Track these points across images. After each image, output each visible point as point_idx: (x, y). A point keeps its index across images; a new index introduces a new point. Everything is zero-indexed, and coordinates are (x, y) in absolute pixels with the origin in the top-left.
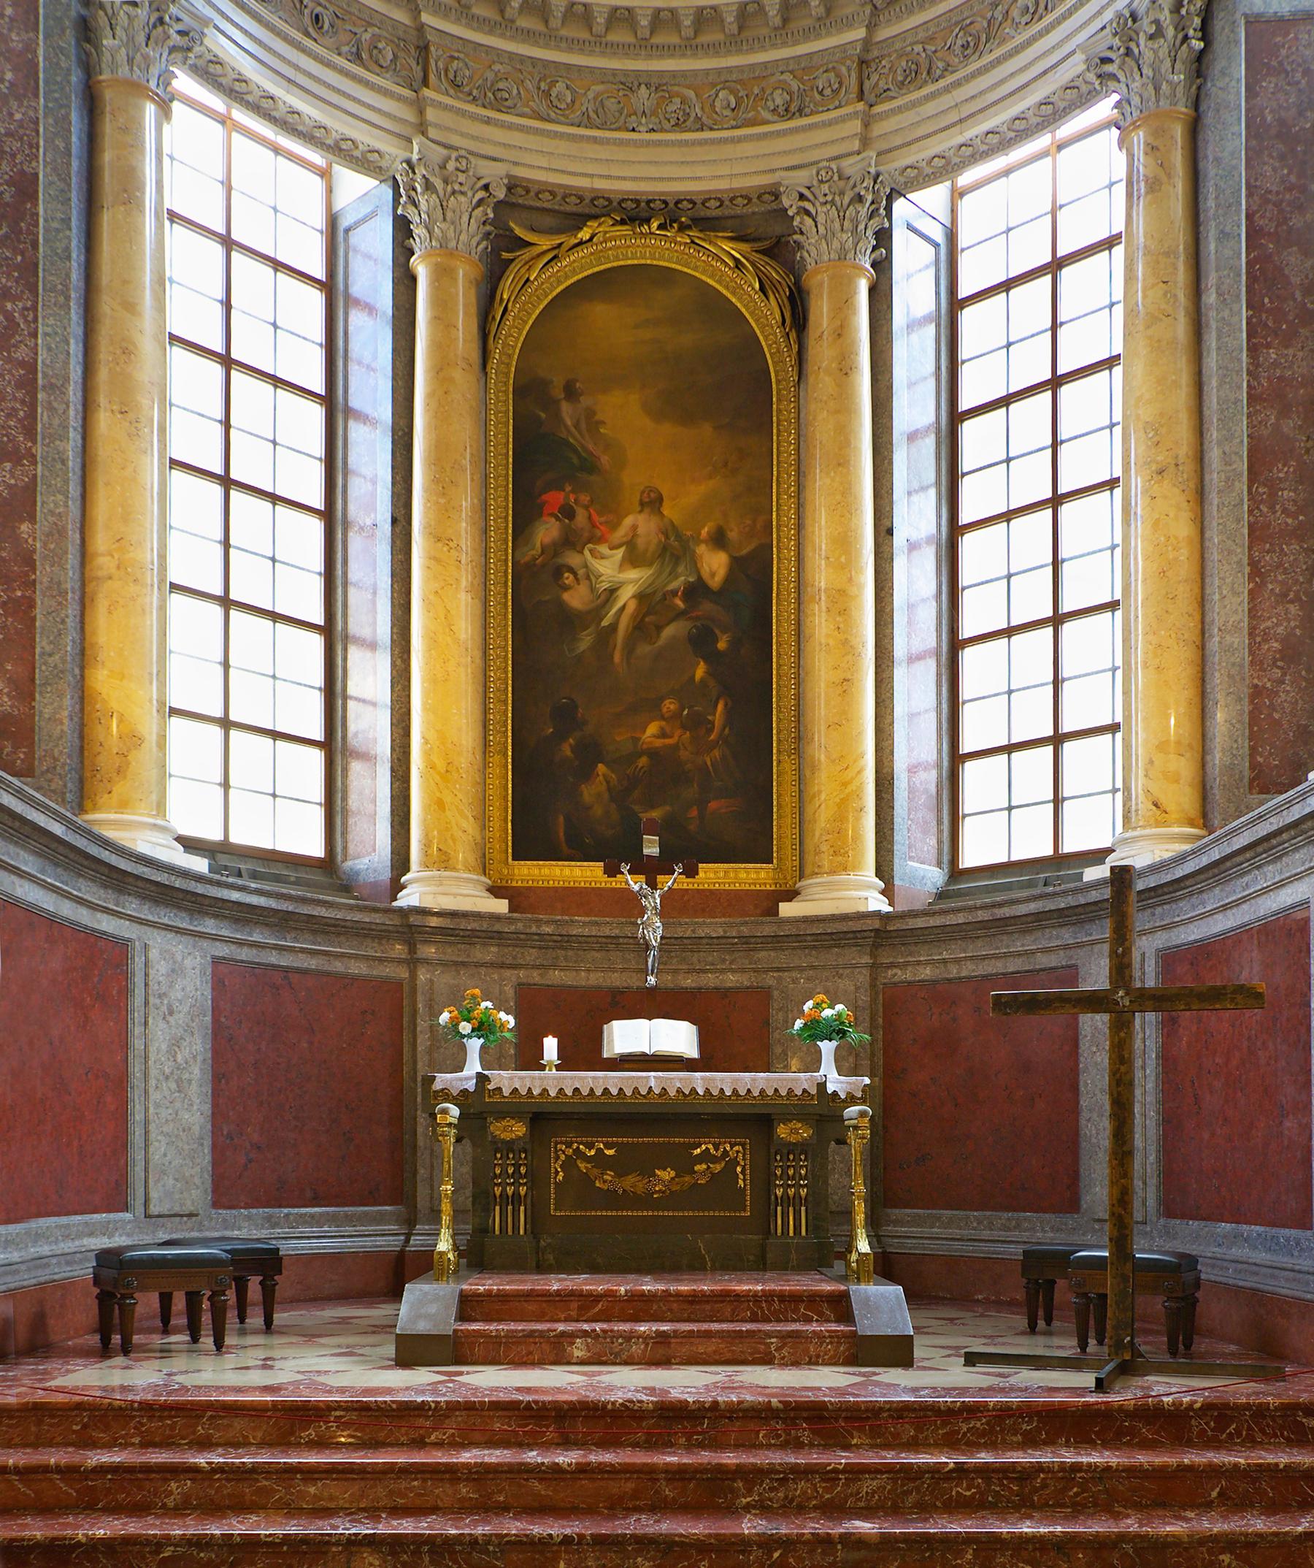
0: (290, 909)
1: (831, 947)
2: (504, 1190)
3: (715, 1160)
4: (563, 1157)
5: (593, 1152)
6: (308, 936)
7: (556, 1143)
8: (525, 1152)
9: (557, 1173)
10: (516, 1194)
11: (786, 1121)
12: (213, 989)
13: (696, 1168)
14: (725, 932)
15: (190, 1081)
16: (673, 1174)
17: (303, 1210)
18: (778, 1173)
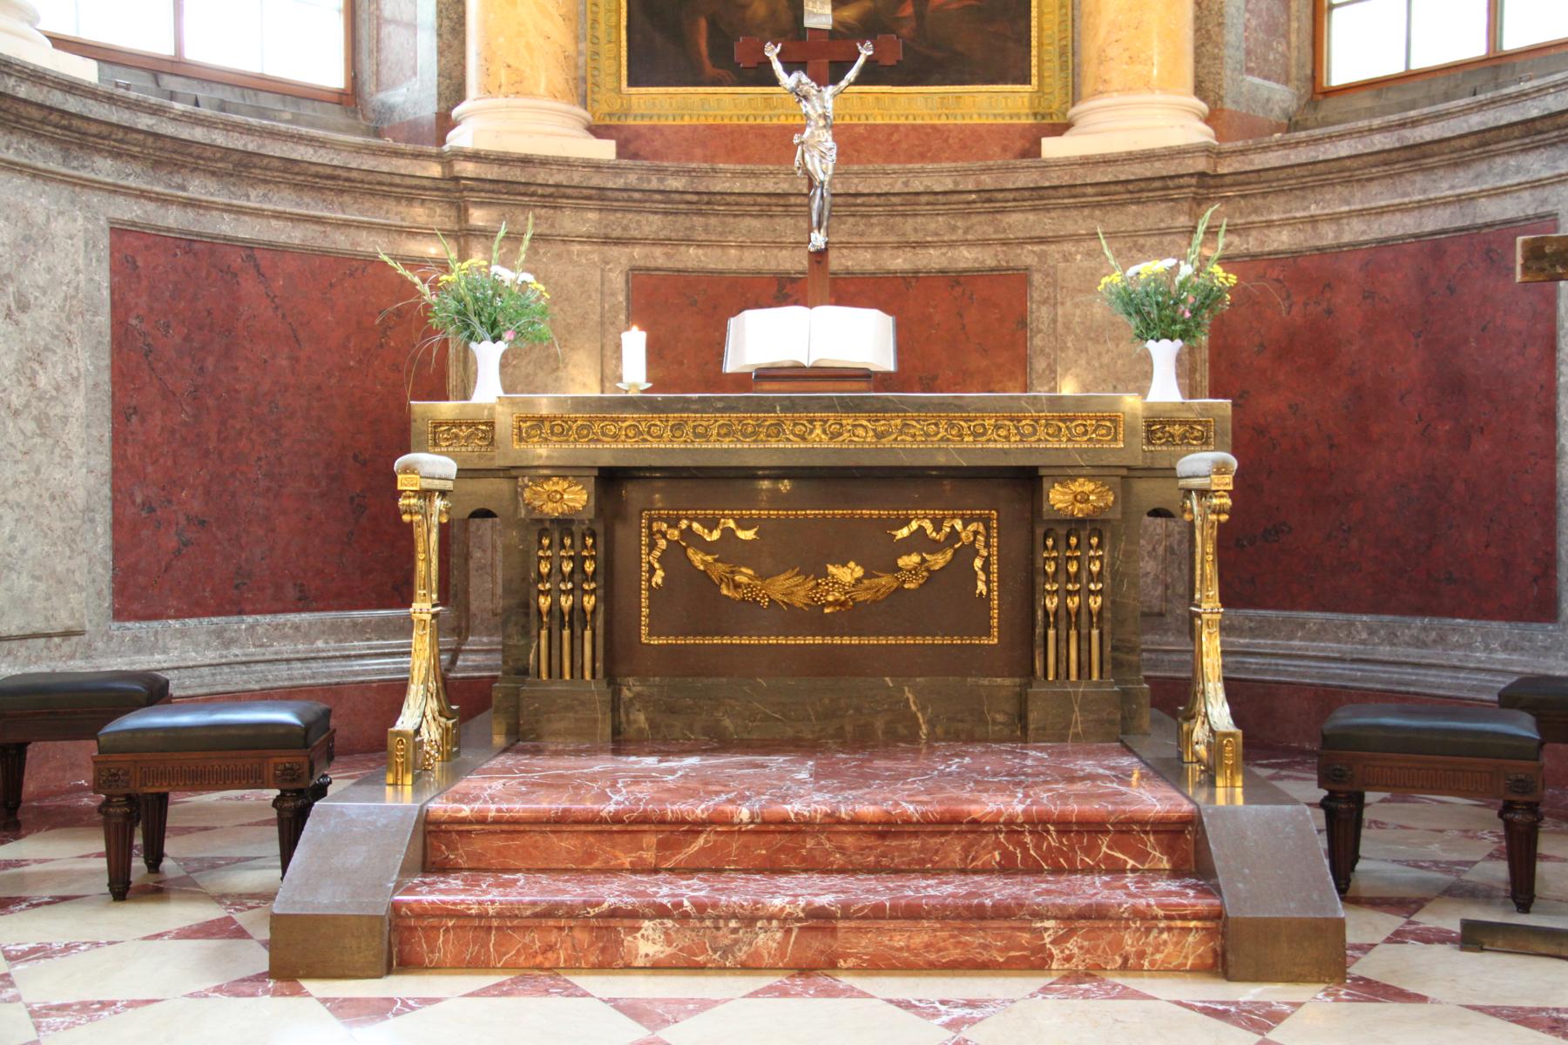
0: (251, 147)
1: (1124, 204)
2: (555, 602)
3: (935, 547)
4: (662, 544)
5: (716, 535)
6: (288, 194)
7: (651, 520)
8: (593, 535)
9: (652, 571)
10: (577, 609)
11: (1066, 474)
12: (113, 272)
13: (901, 562)
14: (956, 183)
15: (65, 420)
16: (859, 572)
17: (281, 618)
18: (1050, 568)
